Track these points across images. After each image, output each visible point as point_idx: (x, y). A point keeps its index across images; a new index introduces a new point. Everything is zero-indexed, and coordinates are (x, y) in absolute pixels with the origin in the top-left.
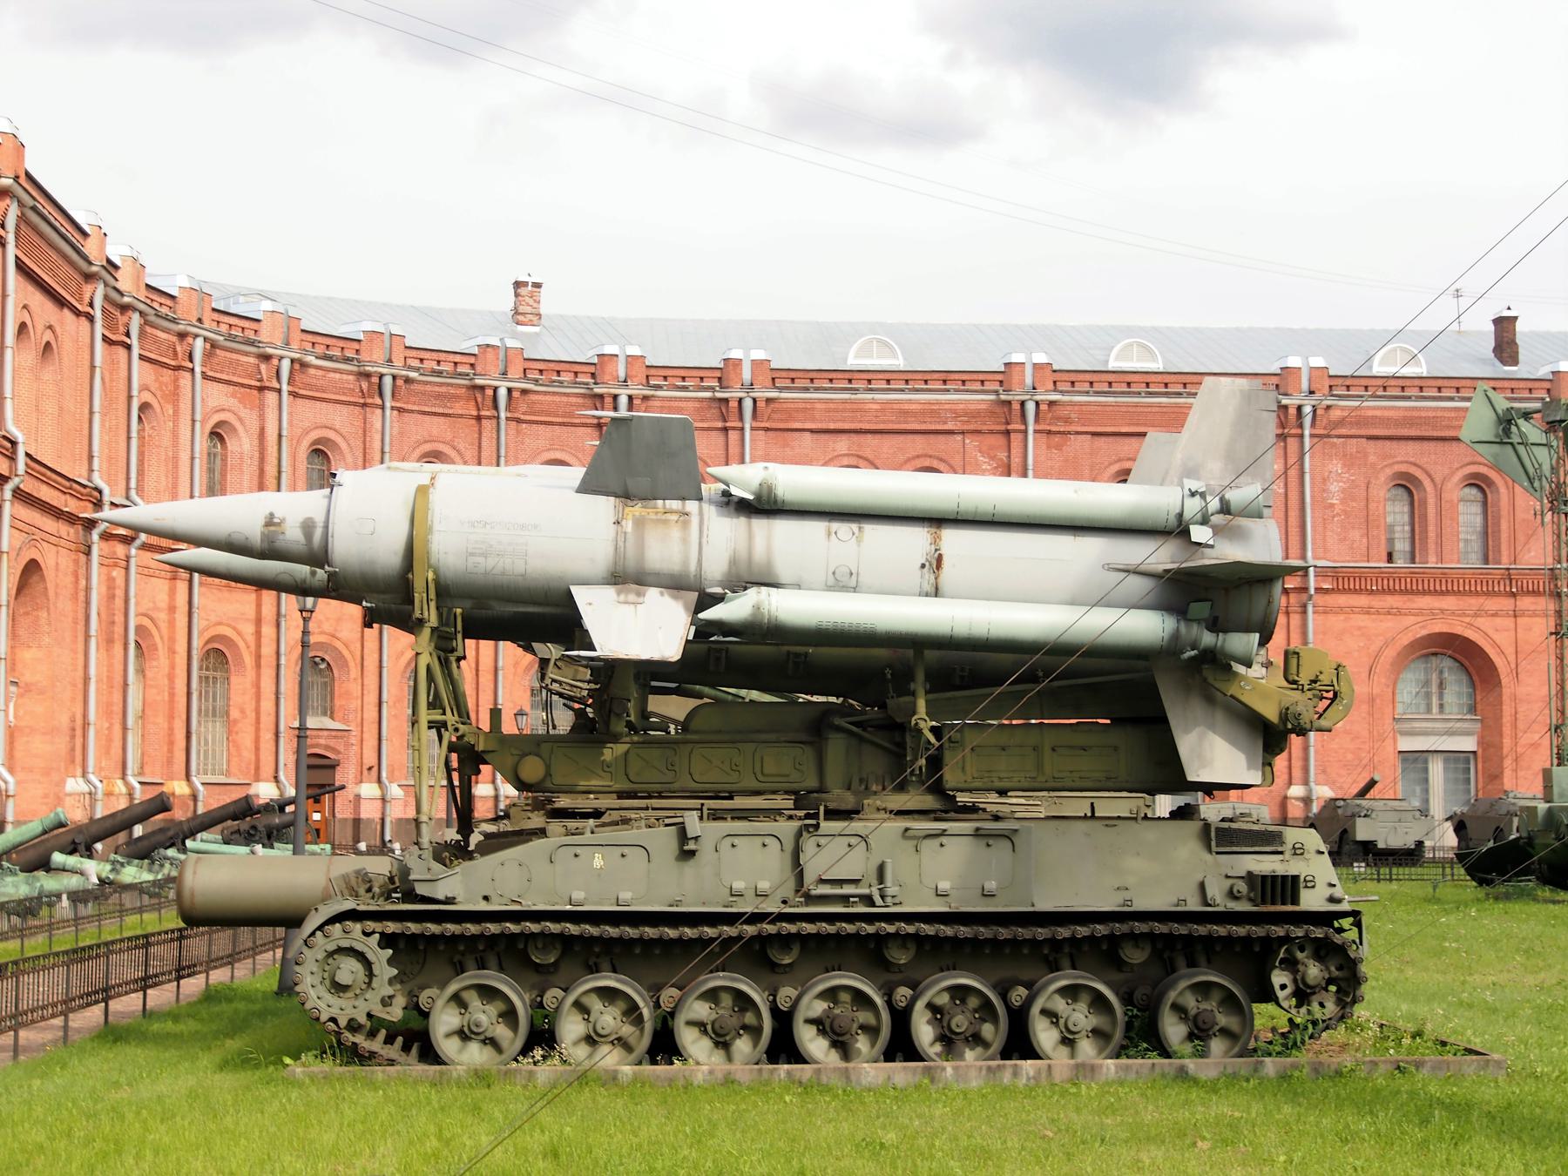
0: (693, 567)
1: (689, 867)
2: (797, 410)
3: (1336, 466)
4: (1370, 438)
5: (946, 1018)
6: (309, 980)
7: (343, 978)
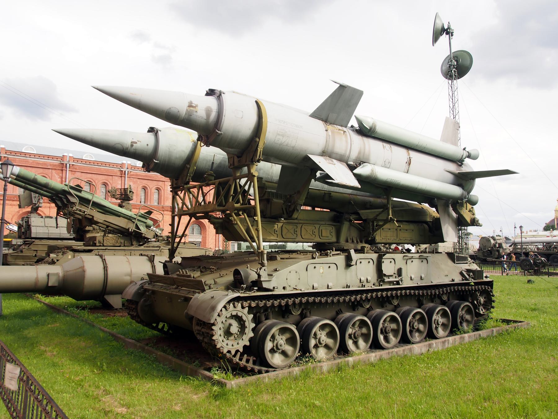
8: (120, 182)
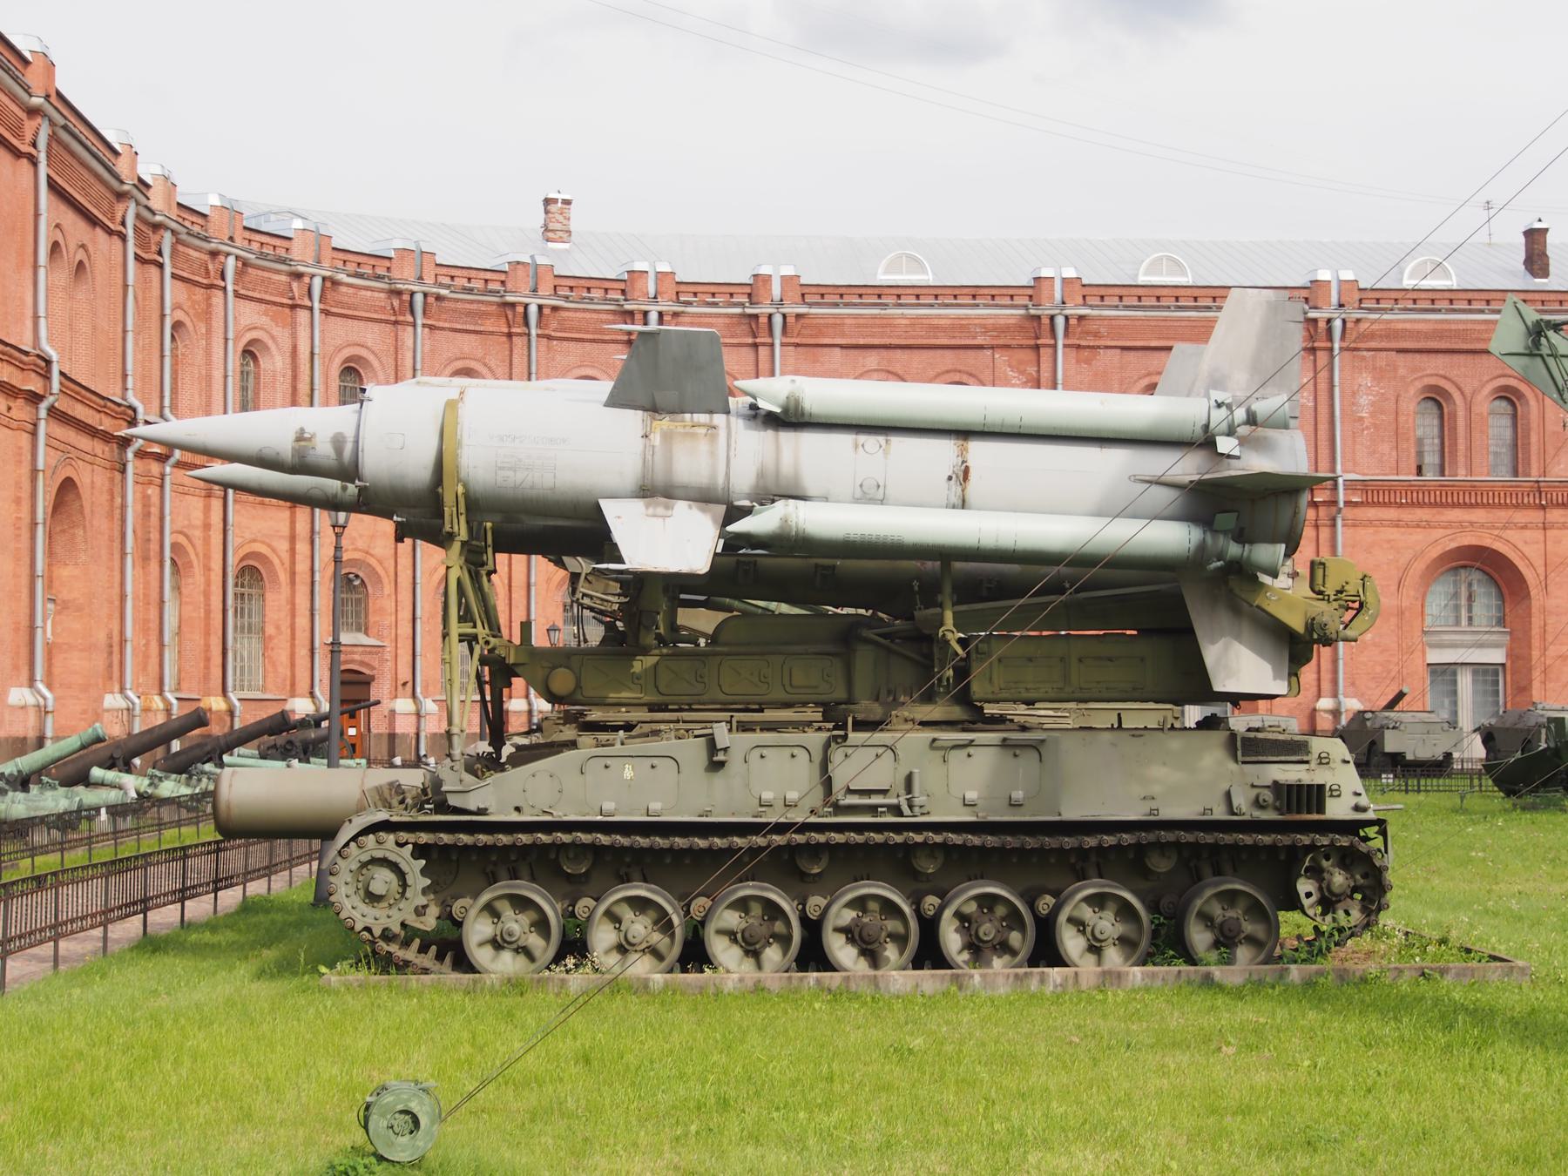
0: (721, 481)
1: (719, 779)
2: (827, 326)
3: (1366, 380)
5: (974, 926)
6: (343, 890)
7: (377, 887)
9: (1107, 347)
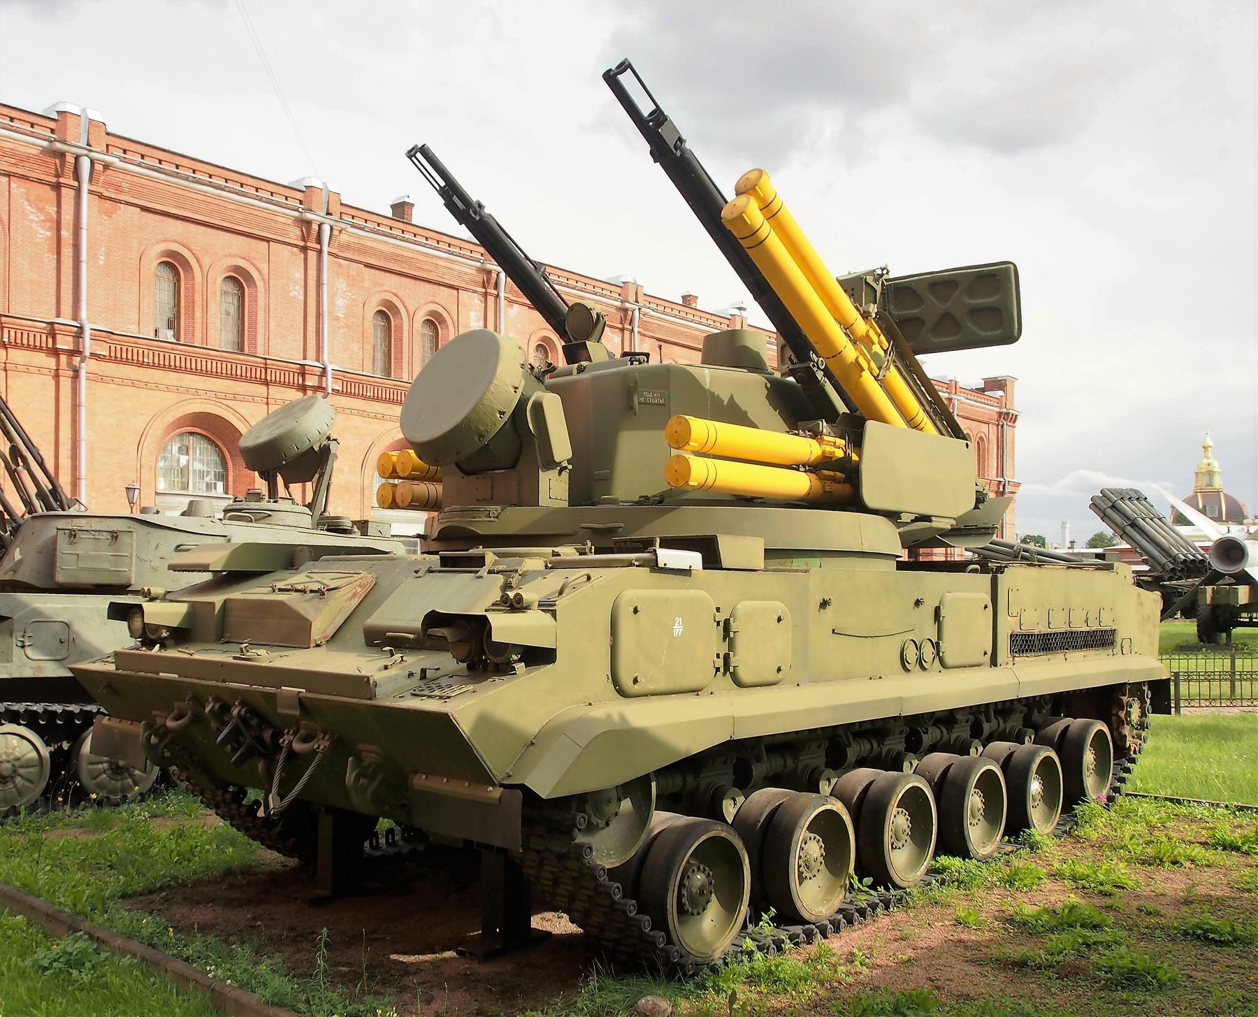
3: (342, 285)
4: (368, 266)
8: (299, 275)
9: (127, 203)
